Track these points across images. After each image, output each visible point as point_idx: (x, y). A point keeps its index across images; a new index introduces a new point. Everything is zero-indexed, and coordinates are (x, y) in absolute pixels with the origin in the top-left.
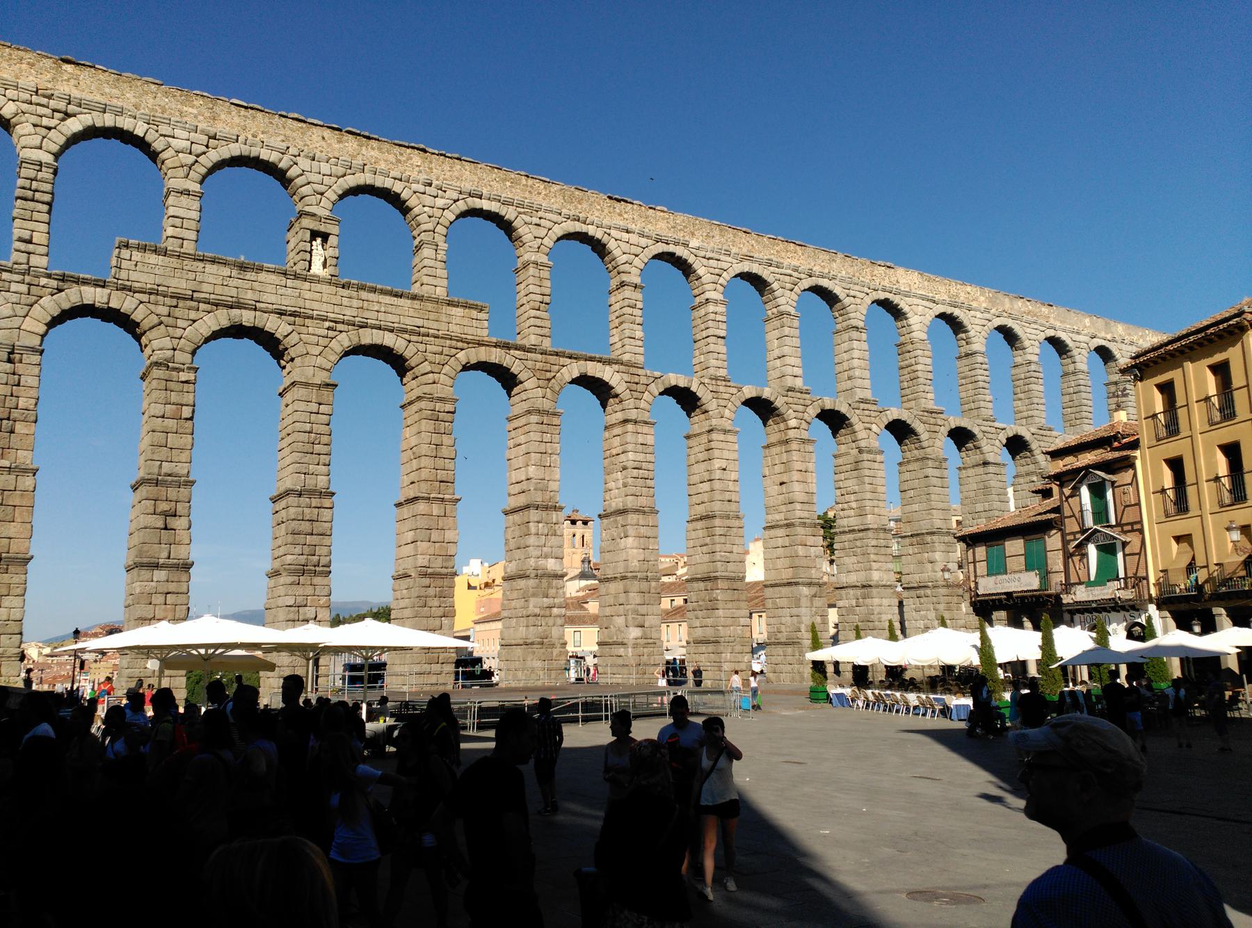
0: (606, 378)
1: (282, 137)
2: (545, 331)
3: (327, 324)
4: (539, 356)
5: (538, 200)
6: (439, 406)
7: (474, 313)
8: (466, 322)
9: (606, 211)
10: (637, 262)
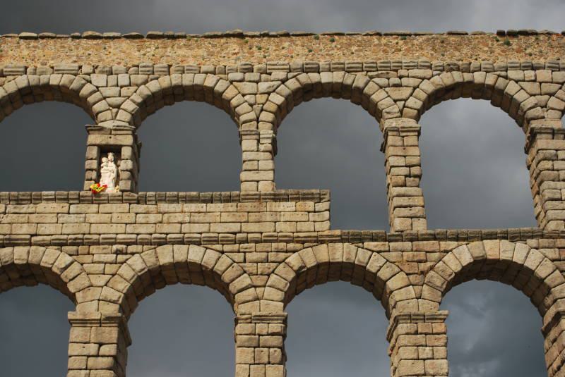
0: (518, 258)
1: (74, 58)
2: (415, 211)
3: (115, 247)
4: (410, 243)
5: (393, 58)
6: (261, 327)
7: (310, 205)
8: (299, 217)
9: (498, 51)
10: (553, 102)
